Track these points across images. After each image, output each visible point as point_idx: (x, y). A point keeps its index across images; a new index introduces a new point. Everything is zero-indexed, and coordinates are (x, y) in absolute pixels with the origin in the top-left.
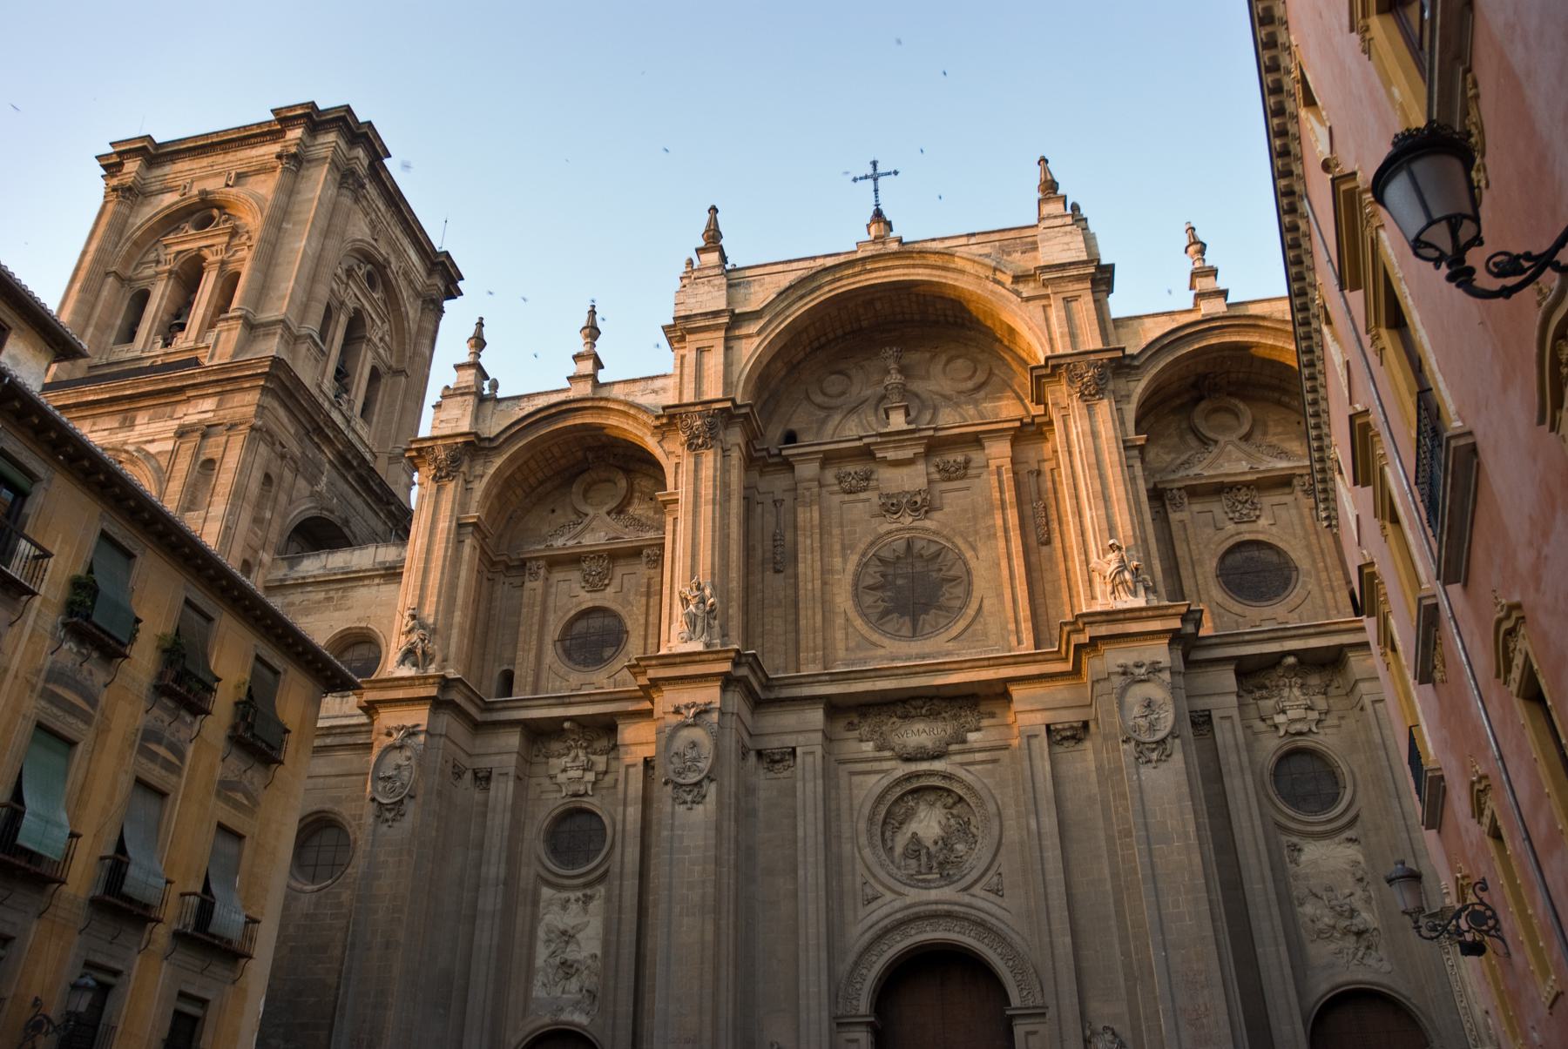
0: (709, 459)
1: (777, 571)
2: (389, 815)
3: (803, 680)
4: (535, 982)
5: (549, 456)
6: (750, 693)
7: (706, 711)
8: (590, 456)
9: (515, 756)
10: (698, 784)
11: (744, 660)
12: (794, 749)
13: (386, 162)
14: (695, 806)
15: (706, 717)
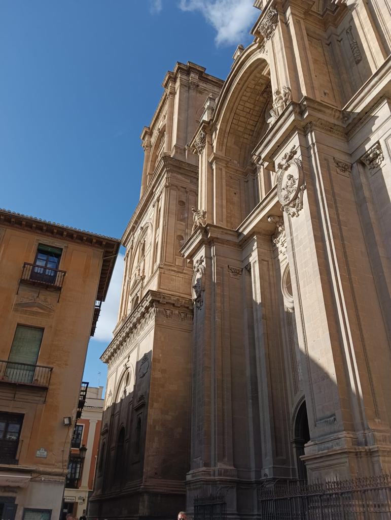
0: (278, 33)
1: (358, 62)
2: (199, 305)
3: (362, 95)
4: (298, 370)
5: (248, 110)
6: (330, 128)
7: (295, 153)
8: (265, 95)
9: (257, 250)
10: (296, 197)
11: (303, 108)
12: (378, 142)
13: (206, 72)
14: (299, 212)
15: (296, 156)
